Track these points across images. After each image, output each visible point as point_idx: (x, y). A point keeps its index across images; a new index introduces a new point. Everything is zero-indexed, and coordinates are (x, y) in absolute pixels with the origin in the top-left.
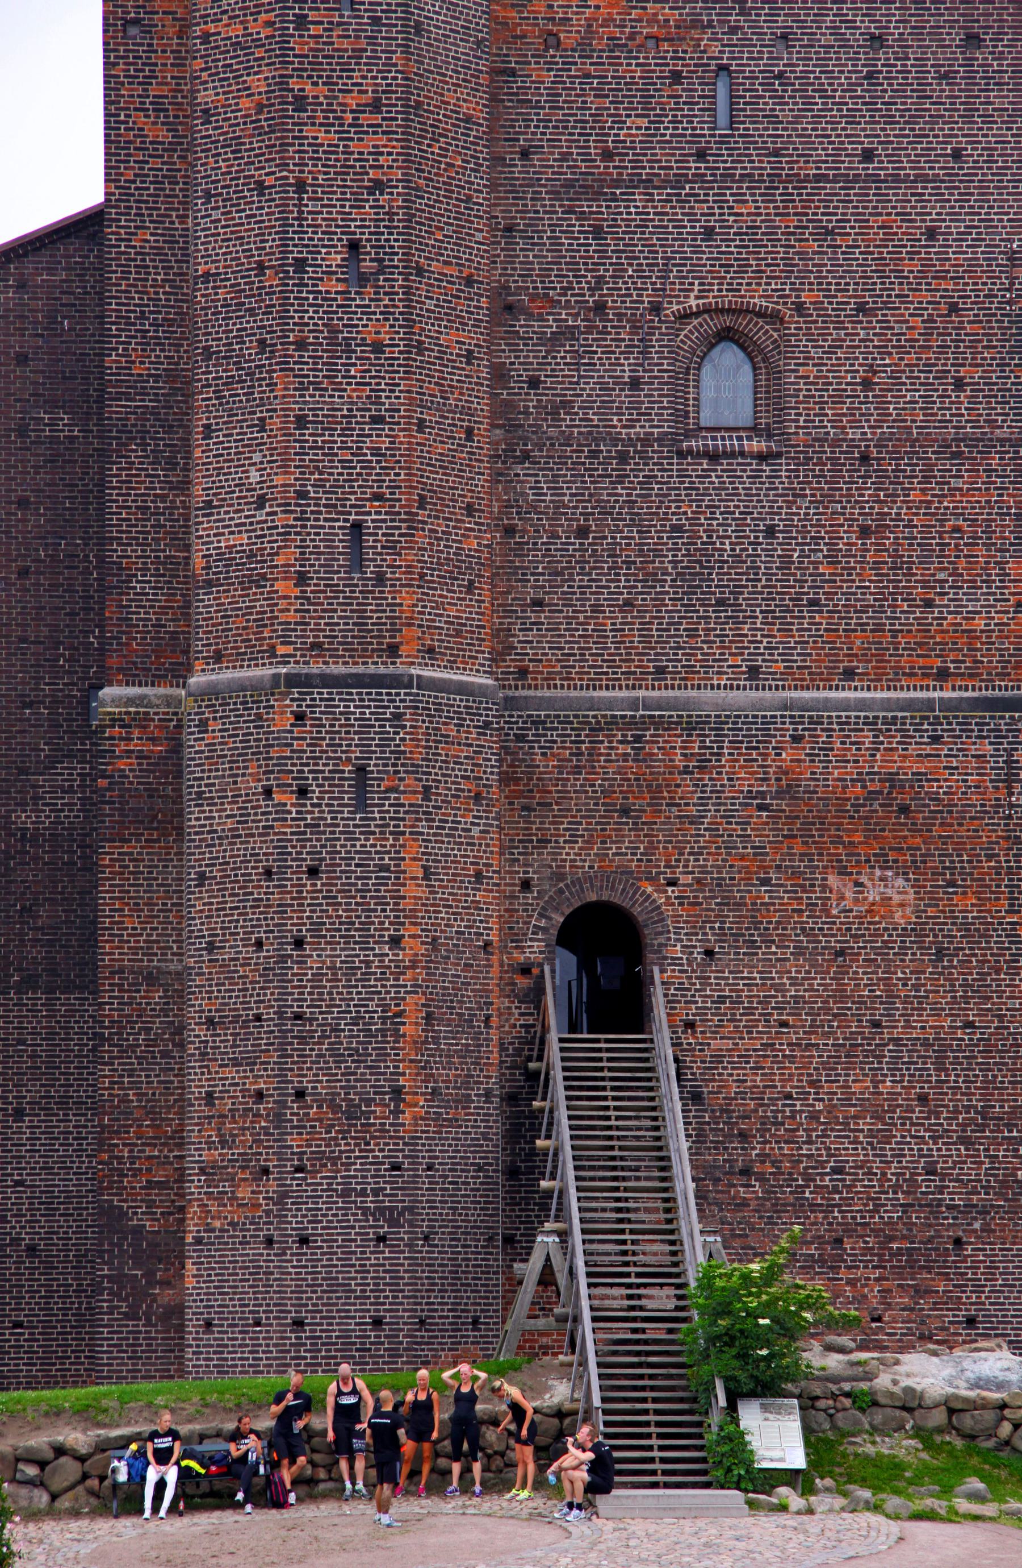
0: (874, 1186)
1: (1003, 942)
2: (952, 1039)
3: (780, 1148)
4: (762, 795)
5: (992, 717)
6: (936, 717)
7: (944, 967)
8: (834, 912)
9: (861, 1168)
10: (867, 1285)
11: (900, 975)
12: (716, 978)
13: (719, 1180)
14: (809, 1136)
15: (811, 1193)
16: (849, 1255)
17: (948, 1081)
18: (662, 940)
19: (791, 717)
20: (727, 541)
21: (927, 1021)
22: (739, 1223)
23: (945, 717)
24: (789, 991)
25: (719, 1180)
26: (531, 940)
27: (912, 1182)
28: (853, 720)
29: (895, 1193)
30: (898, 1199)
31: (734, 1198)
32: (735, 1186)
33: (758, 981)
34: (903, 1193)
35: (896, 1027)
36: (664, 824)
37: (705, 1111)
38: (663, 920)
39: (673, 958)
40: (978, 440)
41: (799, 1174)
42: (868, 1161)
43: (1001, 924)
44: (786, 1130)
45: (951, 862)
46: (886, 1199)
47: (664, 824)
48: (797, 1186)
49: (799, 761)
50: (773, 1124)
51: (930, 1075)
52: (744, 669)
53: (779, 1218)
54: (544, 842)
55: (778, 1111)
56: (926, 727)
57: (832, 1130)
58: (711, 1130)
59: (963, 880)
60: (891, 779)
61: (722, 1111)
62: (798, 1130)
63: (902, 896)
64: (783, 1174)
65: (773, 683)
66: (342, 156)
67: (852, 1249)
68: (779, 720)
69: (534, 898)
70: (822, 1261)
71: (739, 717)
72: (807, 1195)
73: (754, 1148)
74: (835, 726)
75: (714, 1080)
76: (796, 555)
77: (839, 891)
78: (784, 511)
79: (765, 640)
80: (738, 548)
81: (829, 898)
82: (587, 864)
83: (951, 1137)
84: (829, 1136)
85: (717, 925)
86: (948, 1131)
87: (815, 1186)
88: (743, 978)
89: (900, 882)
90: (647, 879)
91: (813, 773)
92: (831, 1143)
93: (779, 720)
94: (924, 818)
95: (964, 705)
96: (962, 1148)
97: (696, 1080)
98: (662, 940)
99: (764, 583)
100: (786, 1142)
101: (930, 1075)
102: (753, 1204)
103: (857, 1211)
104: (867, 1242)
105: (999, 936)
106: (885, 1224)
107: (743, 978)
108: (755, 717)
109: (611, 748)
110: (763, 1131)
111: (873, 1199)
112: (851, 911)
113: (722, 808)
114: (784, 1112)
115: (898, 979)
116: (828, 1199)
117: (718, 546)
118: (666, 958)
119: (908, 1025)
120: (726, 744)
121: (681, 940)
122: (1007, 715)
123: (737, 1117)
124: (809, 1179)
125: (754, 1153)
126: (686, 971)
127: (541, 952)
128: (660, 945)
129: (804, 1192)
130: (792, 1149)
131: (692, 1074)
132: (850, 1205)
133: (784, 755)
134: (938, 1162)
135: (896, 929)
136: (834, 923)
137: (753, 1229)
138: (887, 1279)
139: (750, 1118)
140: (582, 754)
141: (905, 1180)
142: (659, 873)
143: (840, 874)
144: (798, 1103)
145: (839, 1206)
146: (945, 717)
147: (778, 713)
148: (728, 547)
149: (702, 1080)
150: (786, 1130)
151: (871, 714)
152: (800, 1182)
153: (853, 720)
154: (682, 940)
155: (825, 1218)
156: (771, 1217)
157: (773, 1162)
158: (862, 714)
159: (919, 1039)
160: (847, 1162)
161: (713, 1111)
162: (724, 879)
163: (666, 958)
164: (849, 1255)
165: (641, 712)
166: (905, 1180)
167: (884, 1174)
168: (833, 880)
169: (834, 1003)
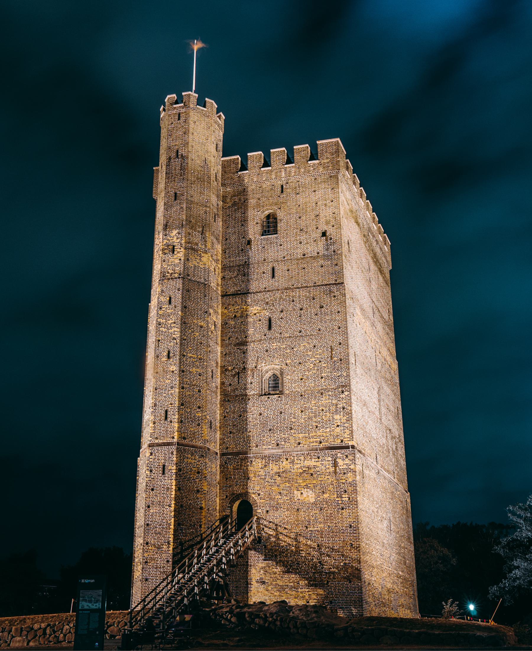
0: (306, 568)
1: (335, 505)
2: (324, 530)
3: (284, 559)
4: (279, 473)
5: (331, 451)
6: (318, 452)
7: (322, 512)
8: (296, 500)
9: (303, 563)
10: (305, 593)
11: (312, 515)
12: (269, 517)
13: (270, 567)
14: (291, 555)
15: (291, 570)
16: (301, 585)
17: (323, 541)
18: (256, 508)
19: (285, 454)
20: (271, 415)
21: (318, 526)
22: (275, 578)
23: (320, 452)
24: (285, 519)
25: (270, 567)
26: (227, 509)
27: (316, 567)
28: (299, 454)
29: (311, 569)
30: (312, 571)
31: (273, 571)
32: (273, 568)
33: (279, 517)
34: (313, 569)
35: (311, 527)
36: (257, 480)
37: (267, 550)
38: (257, 503)
39: (259, 513)
40: (326, 389)
41: (289, 565)
42: (305, 561)
43: (335, 501)
44: (285, 554)
45: (323, 486)
46: (309, 571)
47: (257, 480)
48: (288, 568)
49: (287, 464)
50: (282, 553)
51: (319, 539)
52: (275, 444)
53: (284, 576)
54: (230, 486)
55: (283, 549)
56: (316, 455)
57: (296, 554)
58: (268, 554)
59: (326, 491)
60: (309, 468)
61: (270, 550)
62: (288, 554)
63: (311, 495)
64: (285, 565)
65: (282, 447)
66: (167, 333)
67: (302, 584)
68: (282, 455)
69: (228, 500)
70: (295, 588)
71: (273, 455)
72: (291, 570)
73: (278, 559)
74: (295, 456)
75: (269, 542)
76: (286, 417)
77: (297, 495)
78: (284, 408)
79: (280, 437)
80: (274, 417)
81: (294, 497)
82: (240, 491)
83: (325, 555)
84: (295, 555)
85: (269, 504)
86: (324, 553)
87: (293, 568)
88: (275, 517)
89: (311, 492)
90: (253, 494)
91: (290, 467)
92: (296, 557)
93: (282, 455)
94: (316, 476)
95: (325, 449)
96: (327, 557)
97: (264, 542)
98: (256, 508)
99: (279, 424)
100: (286, 557)
101: (319, 539)
102: (278, 573)
103: (303, 574)
104: (305, 582)
105: (335, 504)
106: (309, 577)
107: (275, 517)
108: (277, 454)
109: (245, 464)
110: (280, 555)
111: (306, 571)
112: (300, 499)
113: (270, 476)
114: (285, 549)
115: (311, 516)
116: (296, 571)
117: (269, 417)
118: (257, 513)
119: (314, 527)
120: (271, 461)
121: (261, 508)
122: (335, 451)
123: (274, 551)
124: (291, 566)
125: (278, 560)
126: (262, 516)
127: (229, 512)
128: (256, 510)
129: (290, 570)
130: (287, 559)
131: (264, 541)
132: (301, 573)
133: (284, 463)
134: (322, 561)
135: (310, 503)
136: (296, 502)
137: (278, 579)
138: (310, 592)
139: (277, 551)
140: (239, 465)
141: (314, 566)
142: (256, 492)
143: (297, 490)
144: (288, 547)
145: (298, 573)
146: (320, 452)
147: (282, 453)
148: (271, 417)
149: (266, 542)
150: (285, 554)
151: (303, 452)
152: (289, 567)
153: (299, 454)
154: (261, 508)
155: (295, 576)
156: (282, 576)
157: (282, 562)
158: (301, 453)
159: (316, 530)
160: (300, 562)
161: (268, 550)
162: (270, 493)
163: (257, 513)
164: (301, 585)
165: (252, 455)
166: (314, 566)
167: (309, 564)
168: (296, 492)
169: (296, 522)
